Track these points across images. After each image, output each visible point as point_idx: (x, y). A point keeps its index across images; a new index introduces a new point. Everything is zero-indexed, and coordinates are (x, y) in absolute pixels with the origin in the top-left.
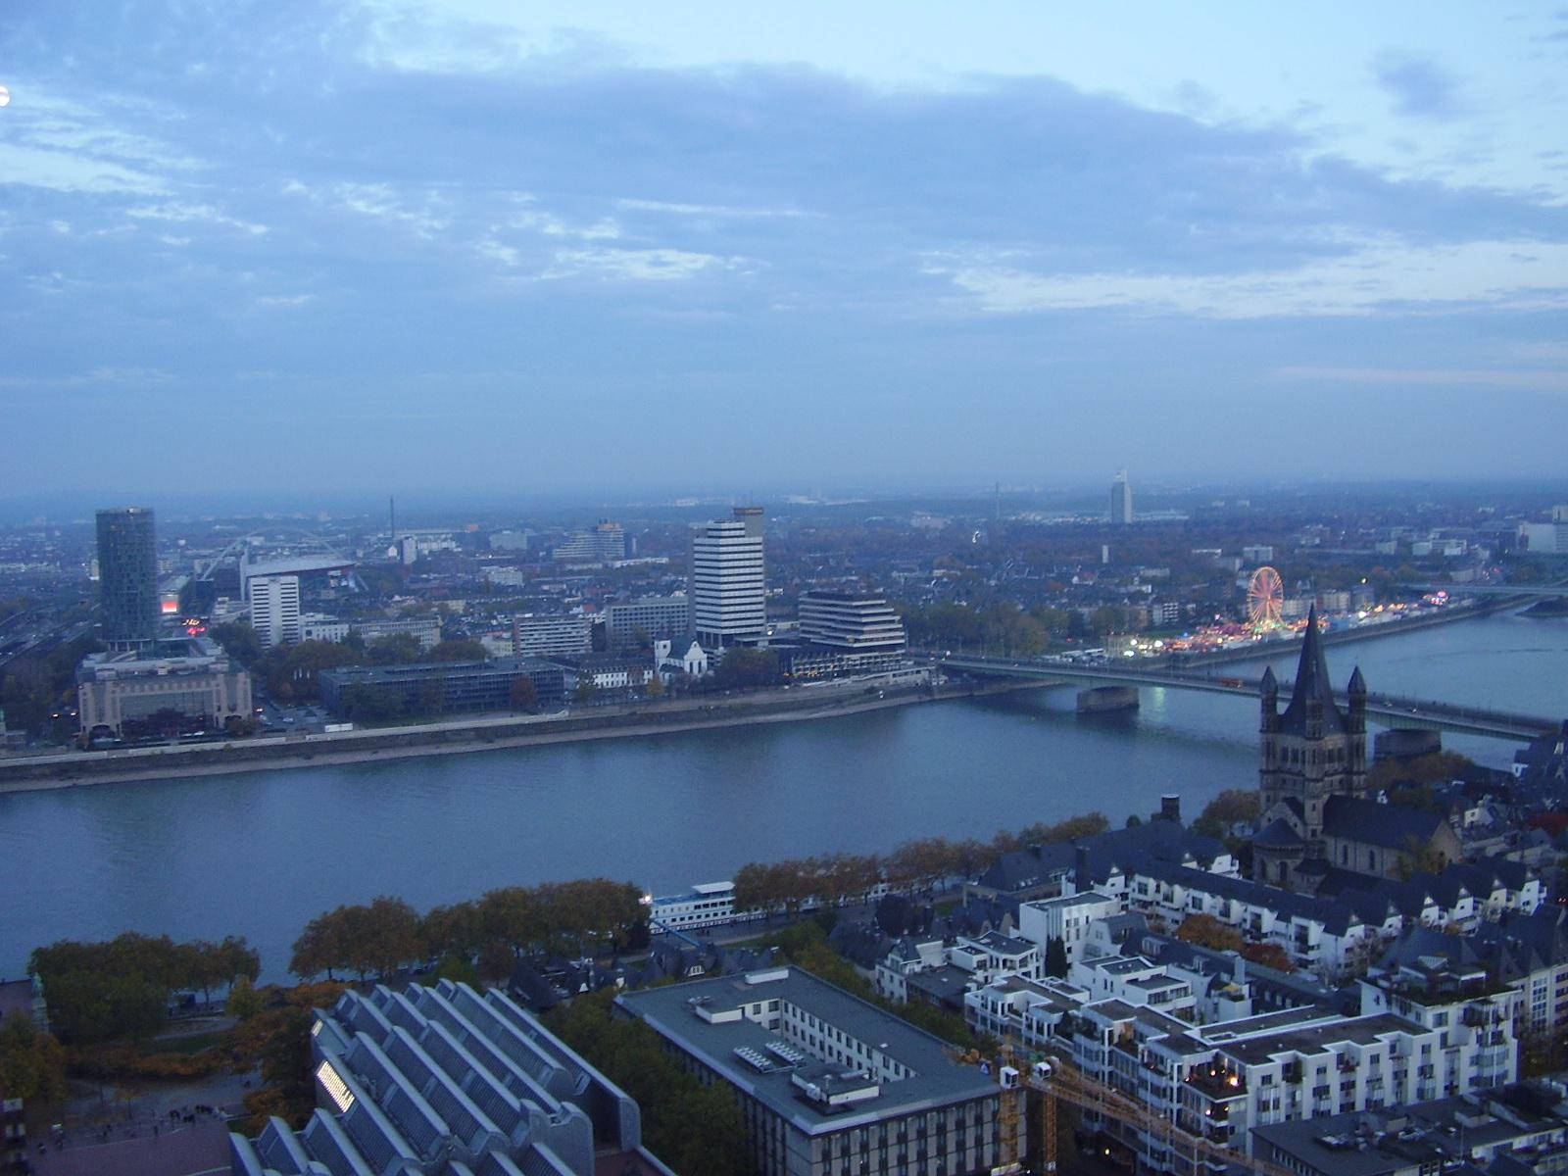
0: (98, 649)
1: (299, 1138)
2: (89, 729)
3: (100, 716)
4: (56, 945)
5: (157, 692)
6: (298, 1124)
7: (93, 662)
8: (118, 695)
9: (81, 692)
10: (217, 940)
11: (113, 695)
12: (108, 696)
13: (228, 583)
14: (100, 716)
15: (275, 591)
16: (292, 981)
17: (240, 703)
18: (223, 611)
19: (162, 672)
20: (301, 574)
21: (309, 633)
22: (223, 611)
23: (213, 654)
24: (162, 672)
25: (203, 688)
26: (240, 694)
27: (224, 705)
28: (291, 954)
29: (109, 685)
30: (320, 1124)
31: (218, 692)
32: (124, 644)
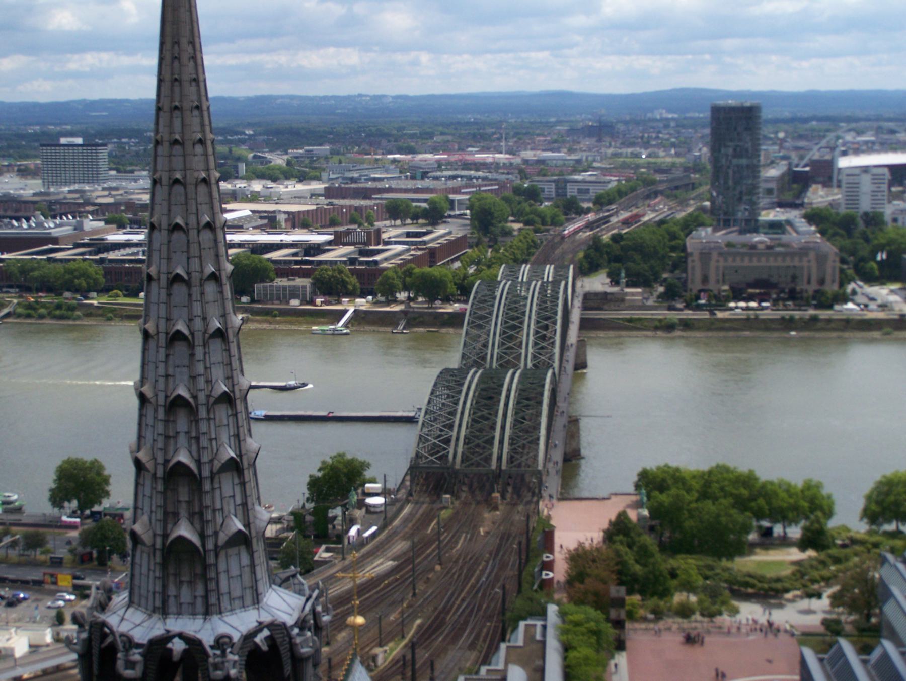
0: (702, 225)
1: (865, 662)
2: (694, 292)
3: (705, 280)
4: (658, 468)
5: (755, 263)
6: (865, 650)
7: (705, 234)
8: (722, 264)
9: (690, 259)
10: (797, 481)
11: (716, 264)
12: (713, 264)
13: (824, 172)
14: (705, 280)
15: (866, 179)
16: (860, 528)
17: (828, 279)
18: (819, 196)
19: (761, 246)
20: (892, 168)
21: (895, 220)
22: (819, 196)
23: (804, 232)
24: (761, 246)
25: (796, 262)
26: (829, 271)
27: (814, 278)
28: (861, 504)
29: (715, 255)
30: (885, 656)
31: (809, 268)
32: (728, 221)
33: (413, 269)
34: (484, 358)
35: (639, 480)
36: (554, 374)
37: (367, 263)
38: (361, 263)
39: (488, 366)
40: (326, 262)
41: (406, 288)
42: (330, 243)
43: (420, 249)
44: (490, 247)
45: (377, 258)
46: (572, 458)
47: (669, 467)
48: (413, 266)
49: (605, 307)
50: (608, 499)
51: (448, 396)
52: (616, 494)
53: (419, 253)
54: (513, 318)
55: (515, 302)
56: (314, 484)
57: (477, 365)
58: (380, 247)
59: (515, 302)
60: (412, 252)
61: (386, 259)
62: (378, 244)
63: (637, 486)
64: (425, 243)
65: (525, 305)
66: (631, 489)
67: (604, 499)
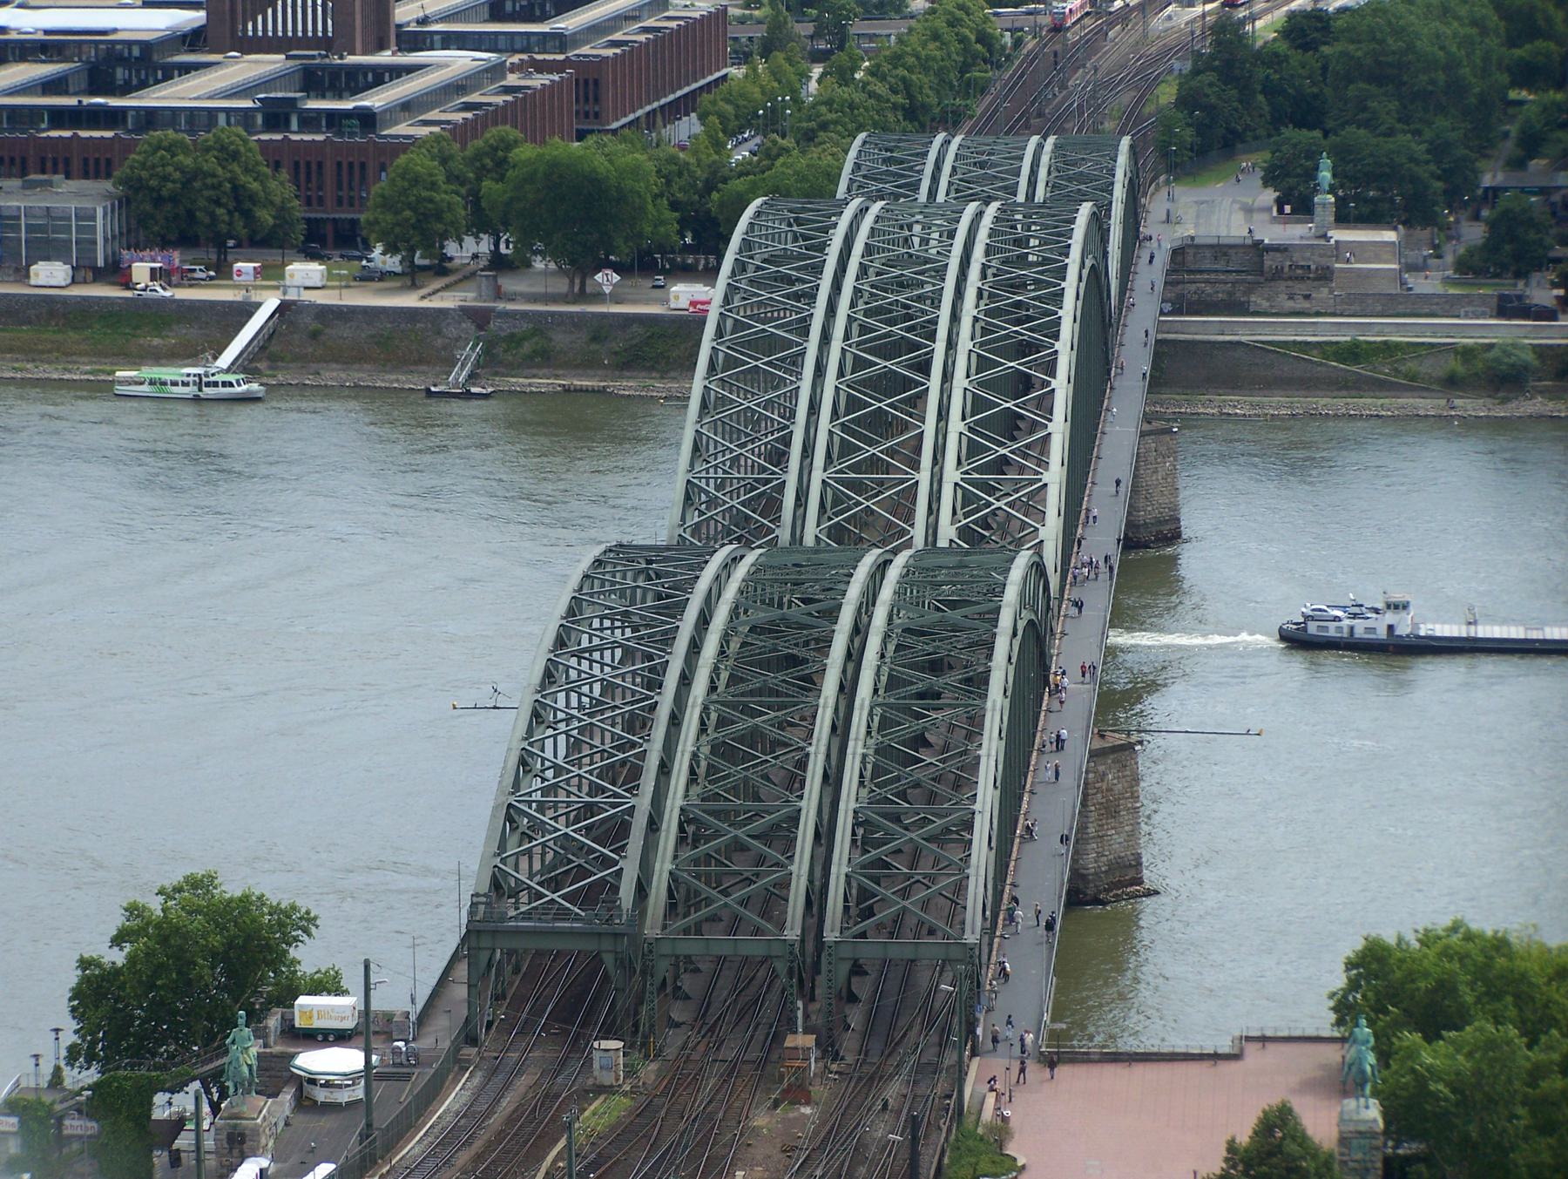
33: (509, 146)
34: (771, 506)
35: (1353, 985)
36: (1038, 568)
37: (334, 119)
38: (310, 121)
39: (784, 534)
40: (170, 116)
41: (480, 223)
42: (193, 39)
43: (541, 67)
44: (817, 57)
45: (374, 100)
46: (1104, 893)
47: (1469, 937)
48: (514, 133)
49: (1258, 300)
50: (1235, 1057)
51: (629, 655)
52: (1264, 1039)
53: (538, 81)
54: (890, 349)
55: (902, 285)
56: (96, 993)
57: (744, 531)
58: (385, 57)
59: (902, 285)
60: (512, 79)
61: (408, 107)
62: (381, 46)
63: (1344, 1010)
64: (561, 41)
65: (936, 301)
66: (1322, 1020)
67: (1216, 1057)
